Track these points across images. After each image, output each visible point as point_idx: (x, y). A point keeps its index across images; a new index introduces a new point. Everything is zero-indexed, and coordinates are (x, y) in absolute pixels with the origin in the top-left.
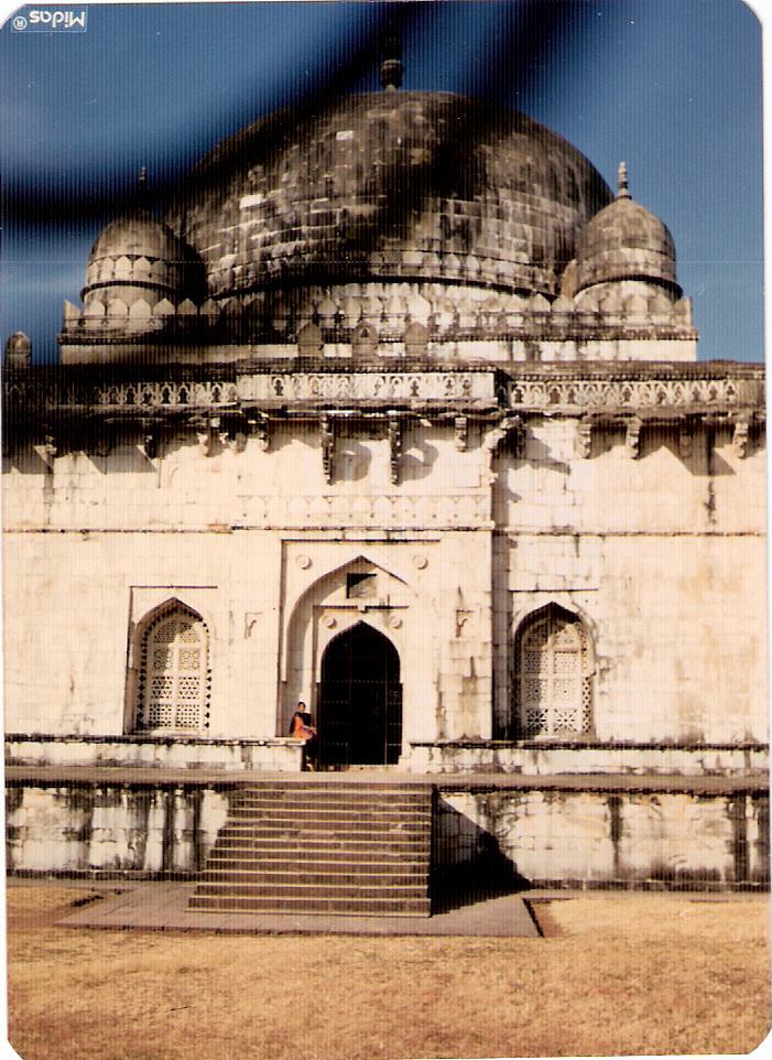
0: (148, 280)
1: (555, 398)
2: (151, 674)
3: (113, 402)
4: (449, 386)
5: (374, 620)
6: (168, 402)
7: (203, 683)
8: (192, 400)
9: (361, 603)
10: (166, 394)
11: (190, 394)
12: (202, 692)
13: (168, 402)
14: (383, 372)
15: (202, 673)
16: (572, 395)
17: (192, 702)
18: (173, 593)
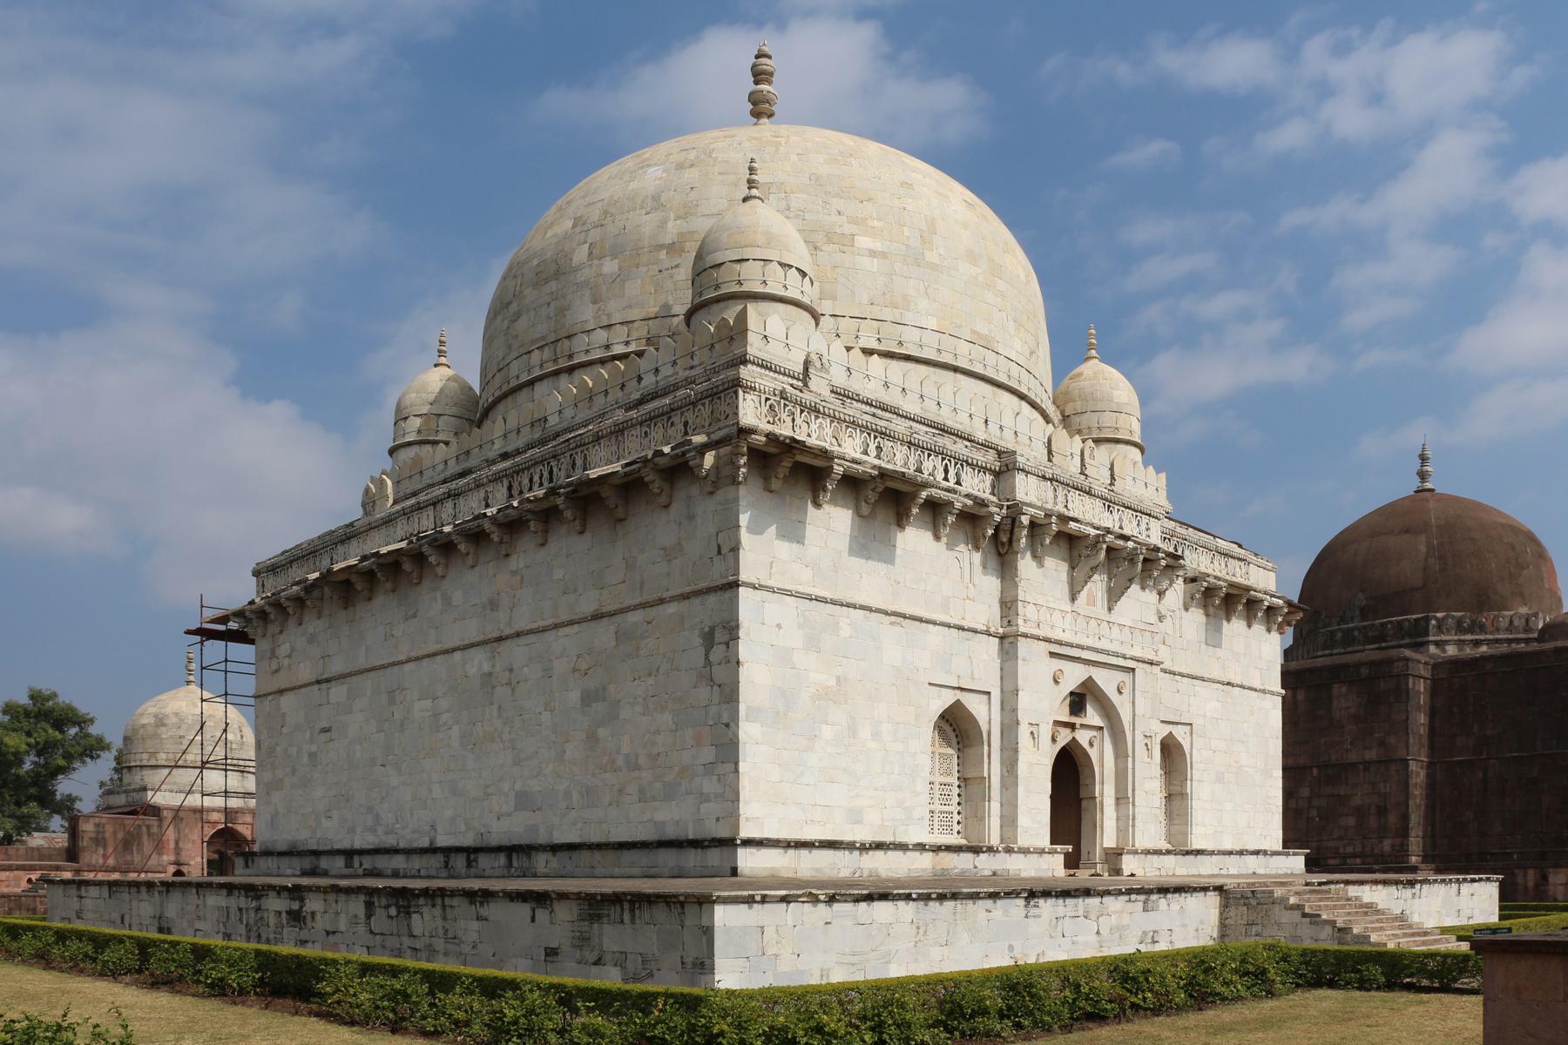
11: (963, 476)
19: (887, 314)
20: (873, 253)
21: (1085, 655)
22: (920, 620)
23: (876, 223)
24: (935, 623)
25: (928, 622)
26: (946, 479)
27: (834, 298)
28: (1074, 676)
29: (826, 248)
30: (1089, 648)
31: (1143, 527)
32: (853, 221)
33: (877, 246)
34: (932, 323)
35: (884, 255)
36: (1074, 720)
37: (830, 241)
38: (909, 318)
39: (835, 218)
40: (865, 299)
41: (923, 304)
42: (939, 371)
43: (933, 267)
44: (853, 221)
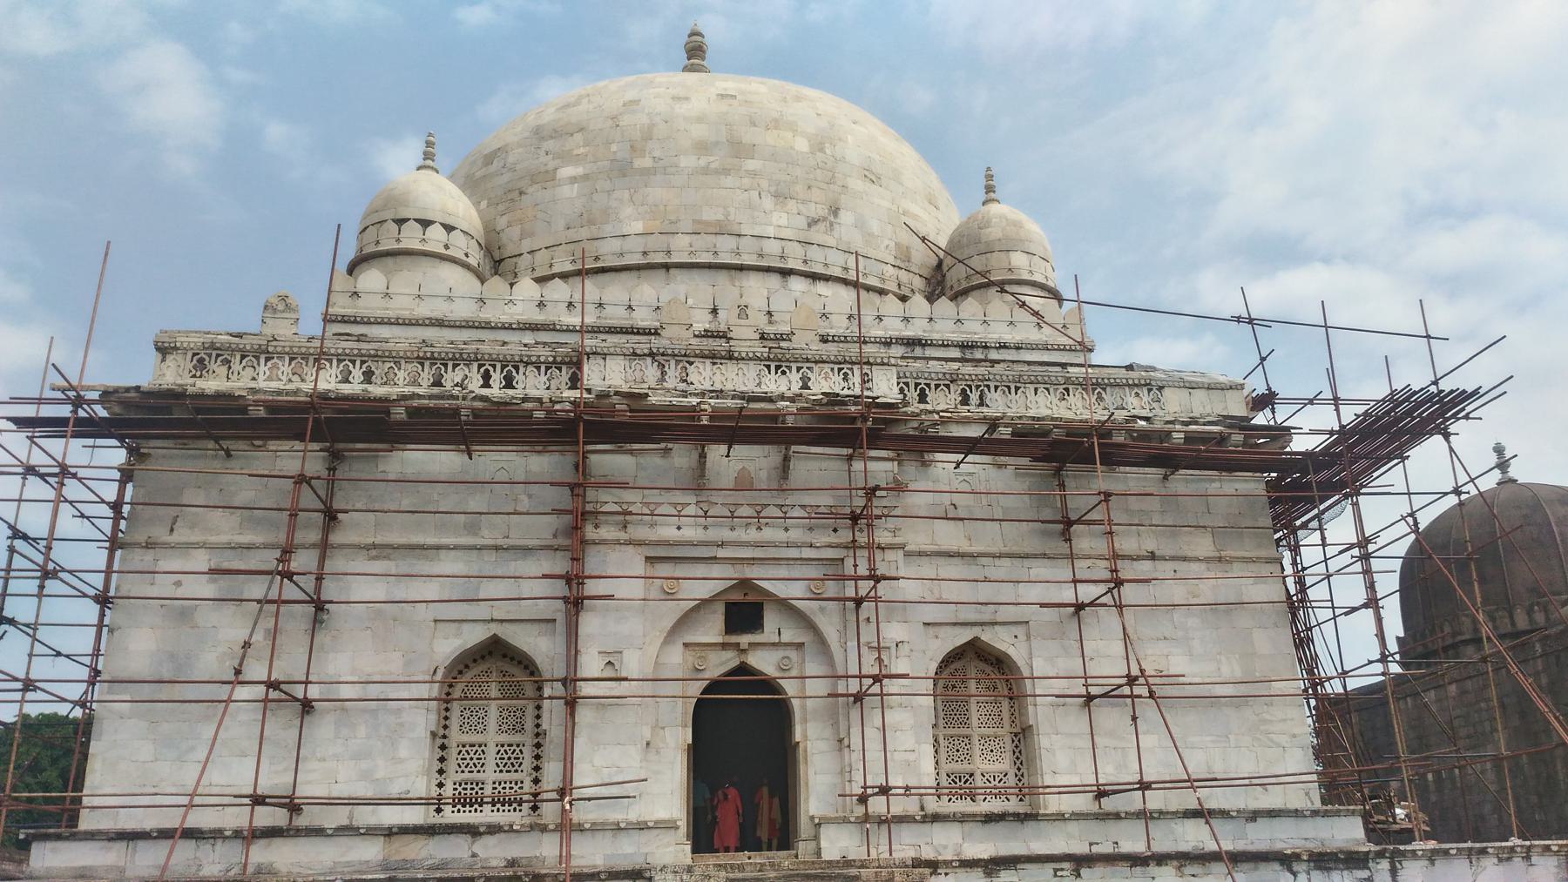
0: (443, 251)
1: (965, 401)
2: (456, 736)
3: (415, 383)
4: (845, 378)
5: (764, 663)
6: (489, 386)
7: (528, 753)
8: (521, 386)
9: (744, 639)
10: (486, 377)
11: (519, 378)
12: (528, 763)
13: (489, 386)
14: (769, 359)
15: (528, 739)
16: (981, 397)
17: (514, 776)
18: (495, 629)
19: (584, 233)
20: (573, 180)
21: (721, 553)
22: (422, 547)
23: (582, 150)
24: (447, 548)
25: (438, 548)
26: (486, 385)
27: (532, 235)
28: (703, 585)
29: (530, 190)
30: (722, 545)
31: (857, 379)
32: (558, 156)
33: (580, 171)
34: (638, 227)
35: (586, 177)
36: (734, 639)
37: (534, 182)
38: (608, 229)
39: (543, 159)
40: (561, 224)
41: (628, 211)
42: (643, 273)
43: (646, 172)
44: (558, 156)
